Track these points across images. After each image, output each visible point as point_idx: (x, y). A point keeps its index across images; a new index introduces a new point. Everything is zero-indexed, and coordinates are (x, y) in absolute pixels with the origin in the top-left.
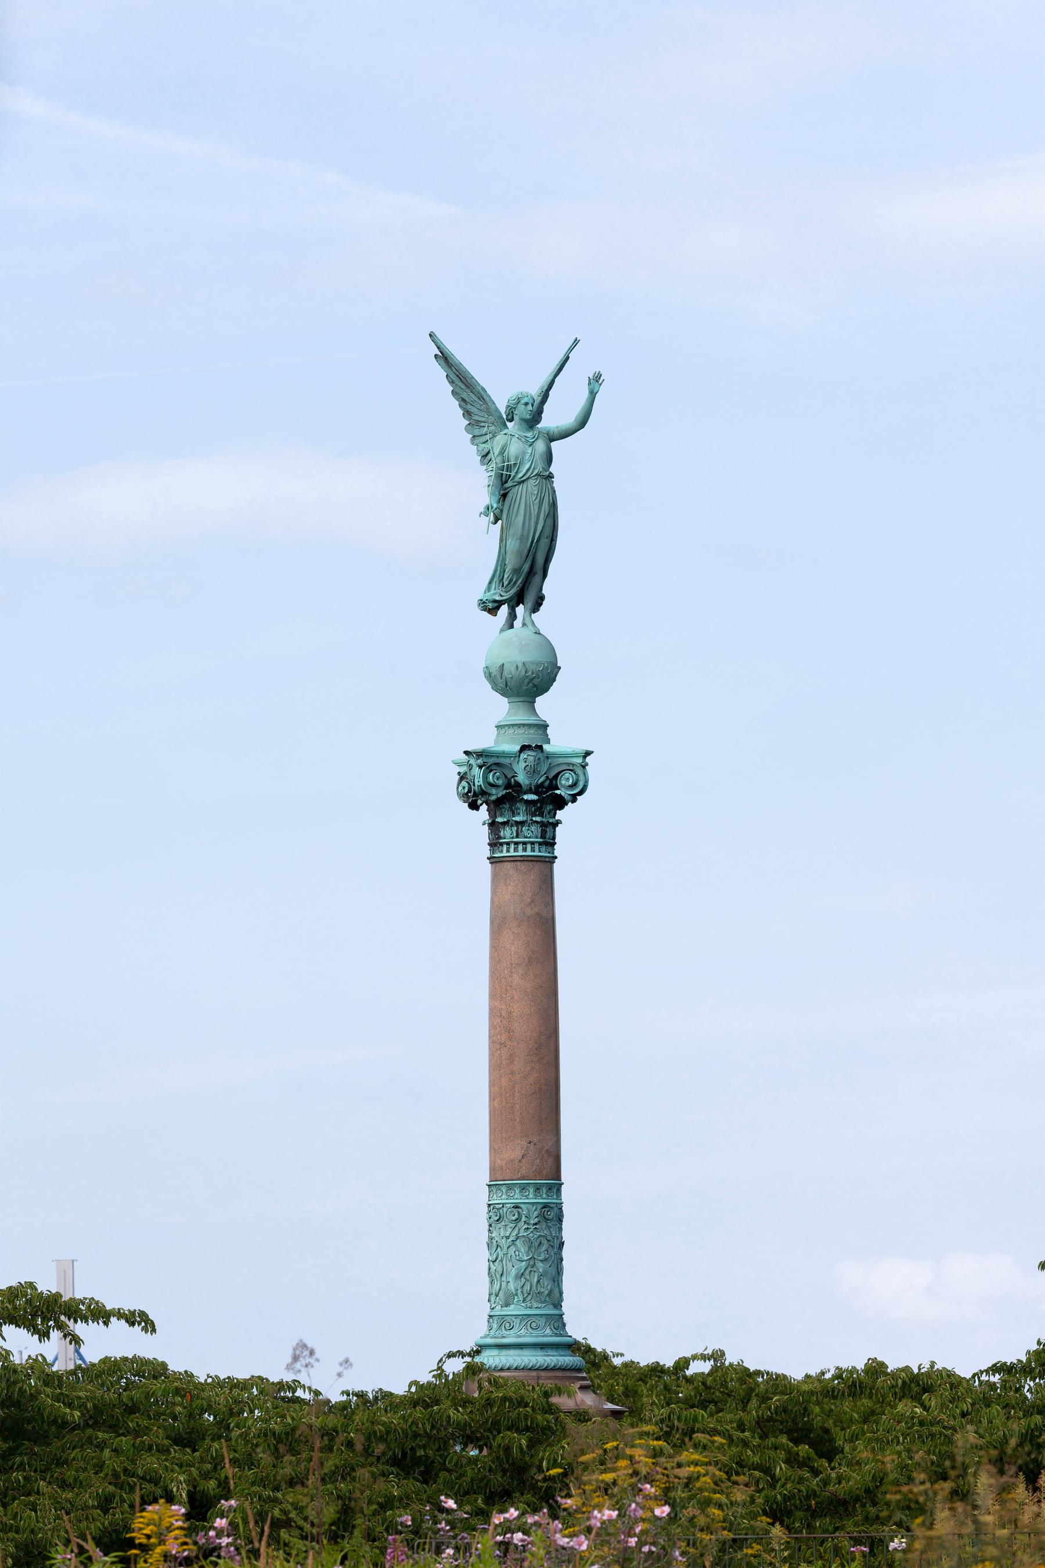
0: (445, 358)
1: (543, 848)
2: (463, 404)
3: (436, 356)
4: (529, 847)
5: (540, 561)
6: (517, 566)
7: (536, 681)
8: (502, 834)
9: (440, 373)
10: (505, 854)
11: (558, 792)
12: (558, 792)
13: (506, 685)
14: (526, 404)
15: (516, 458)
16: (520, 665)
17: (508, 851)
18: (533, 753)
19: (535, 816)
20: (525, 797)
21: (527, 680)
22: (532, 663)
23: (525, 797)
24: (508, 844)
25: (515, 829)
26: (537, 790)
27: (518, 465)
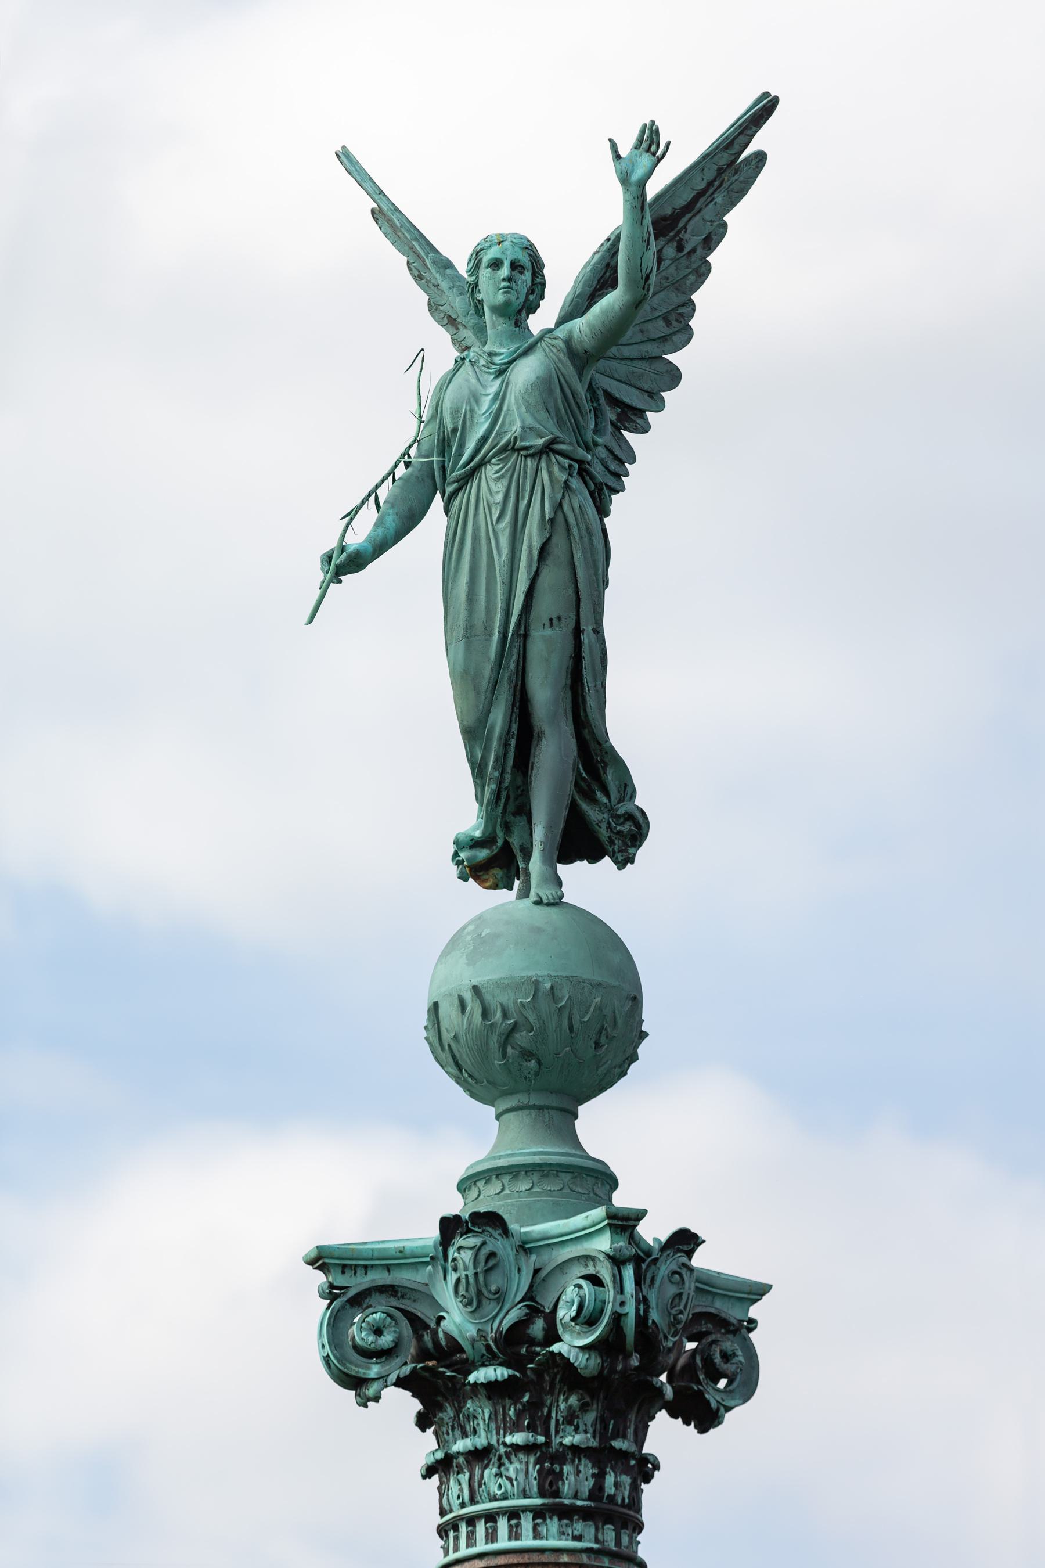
0: (388, 218)
1: (553, 1525)
4: (503, 1524)
5: (544, 692)
6: (470, 721)
7: (522, 1038)
11: (556, 1348)
12: (556, 1348)
14: (496, 264)
15: (455, 412)
16: (468, 996)
18: (471, 1241)
19: (516, 1427)
20: (481, 1375)
21: (494, 1043)
22: (502, 985)
23: (471, 1378)
25: (464, 1478)
26: (511, 1345)
27: (461, 431)
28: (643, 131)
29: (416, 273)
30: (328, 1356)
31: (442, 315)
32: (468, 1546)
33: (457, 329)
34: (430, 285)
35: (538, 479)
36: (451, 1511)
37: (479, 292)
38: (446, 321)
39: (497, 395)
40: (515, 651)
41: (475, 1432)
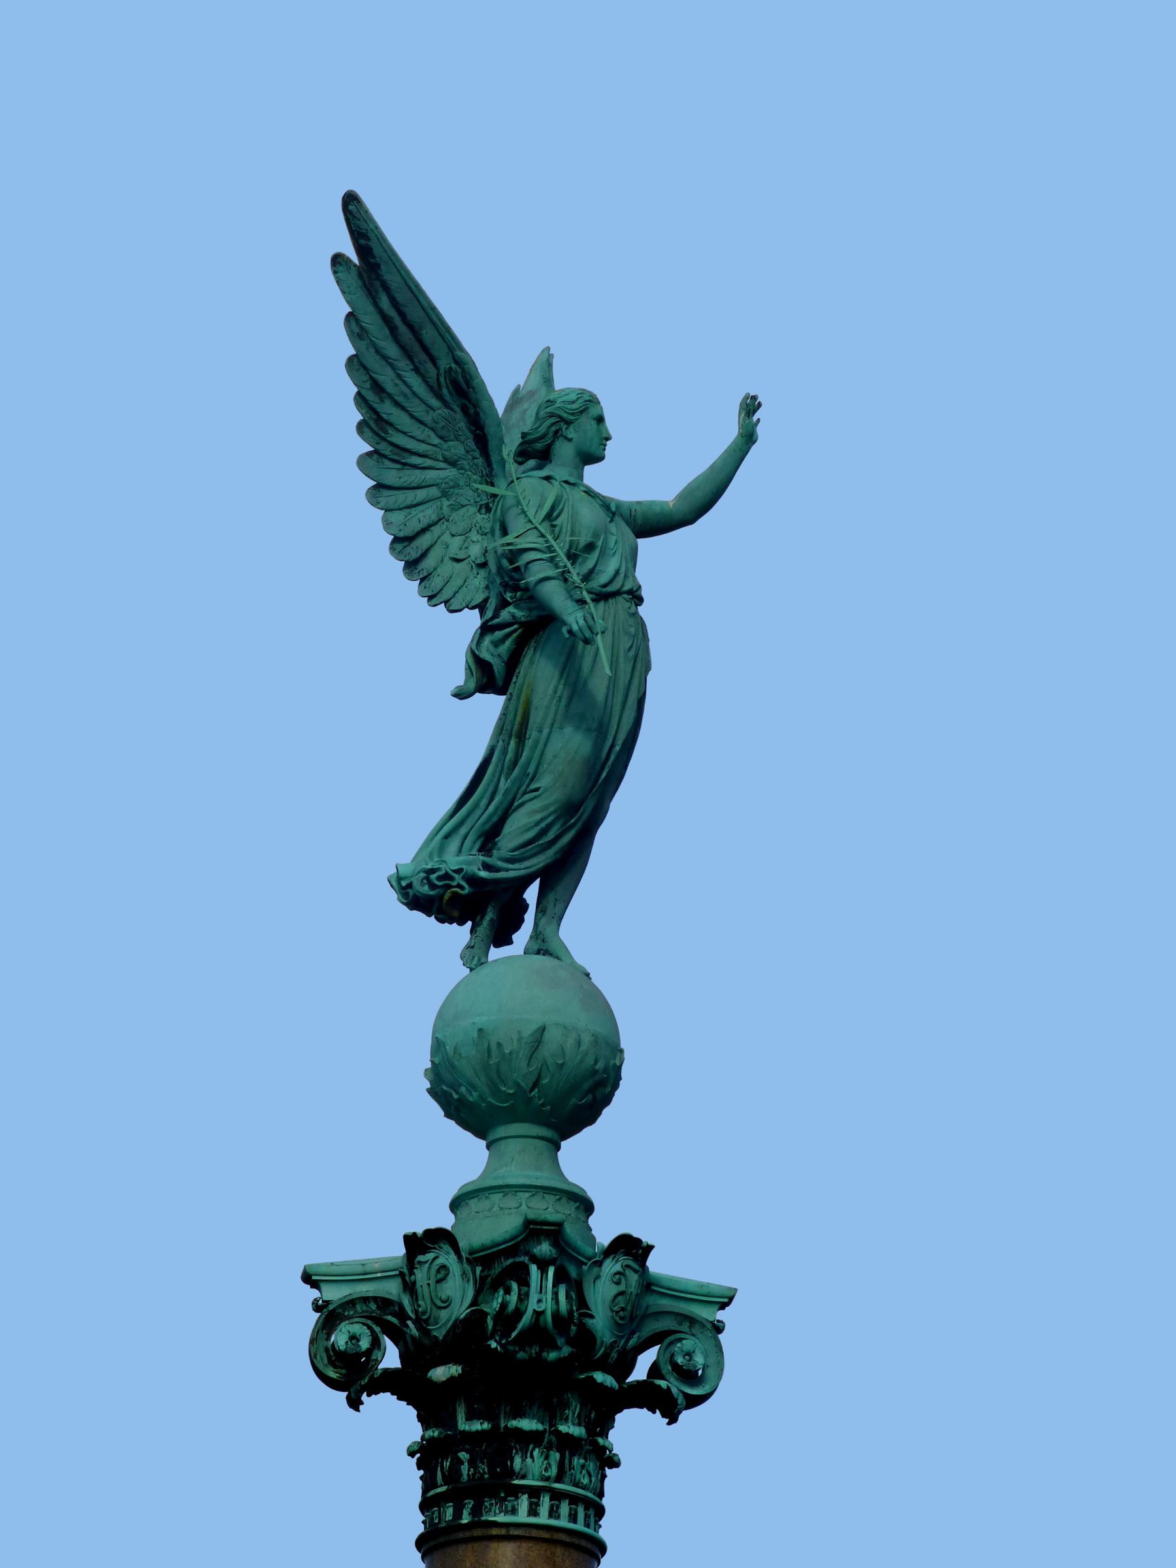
2: (371, 396)
3: (338, 260)
8: (517, 1462)
10: (522, 1517)
13: (536, 1084)
16: (587, 1040)
17: (533, 1512)
24: (534, 1493)
25: (555, 1456)
30: (543, 1312)
32: (550, 1516)
33: (382, 401)
34: (372, 350)
36: (524, 1477)
41: (567, 1419)
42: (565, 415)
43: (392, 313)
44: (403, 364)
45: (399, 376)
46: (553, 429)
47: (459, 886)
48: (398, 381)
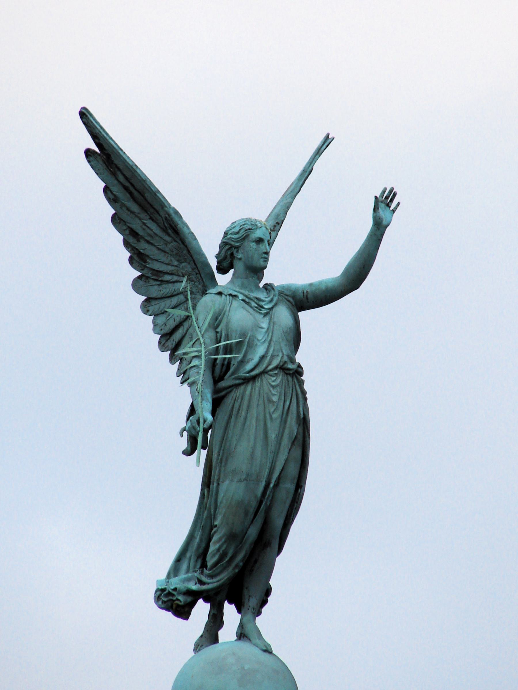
9: (92, 184)
28: (384, 192)
29: (112, 197)
31: (125, 228)
33: (138, 241)
34: (124, 209)
35: (294, 390)
37: (237, 251)
38: (127, 232)
39: (268, 329)
40: (271, 494)
42: (233, 243)
43: (127, 184)
44: (143, 215)
45: (144, 224)
46: (229, 253)
47: (178, 600)
48: (144, 227)
